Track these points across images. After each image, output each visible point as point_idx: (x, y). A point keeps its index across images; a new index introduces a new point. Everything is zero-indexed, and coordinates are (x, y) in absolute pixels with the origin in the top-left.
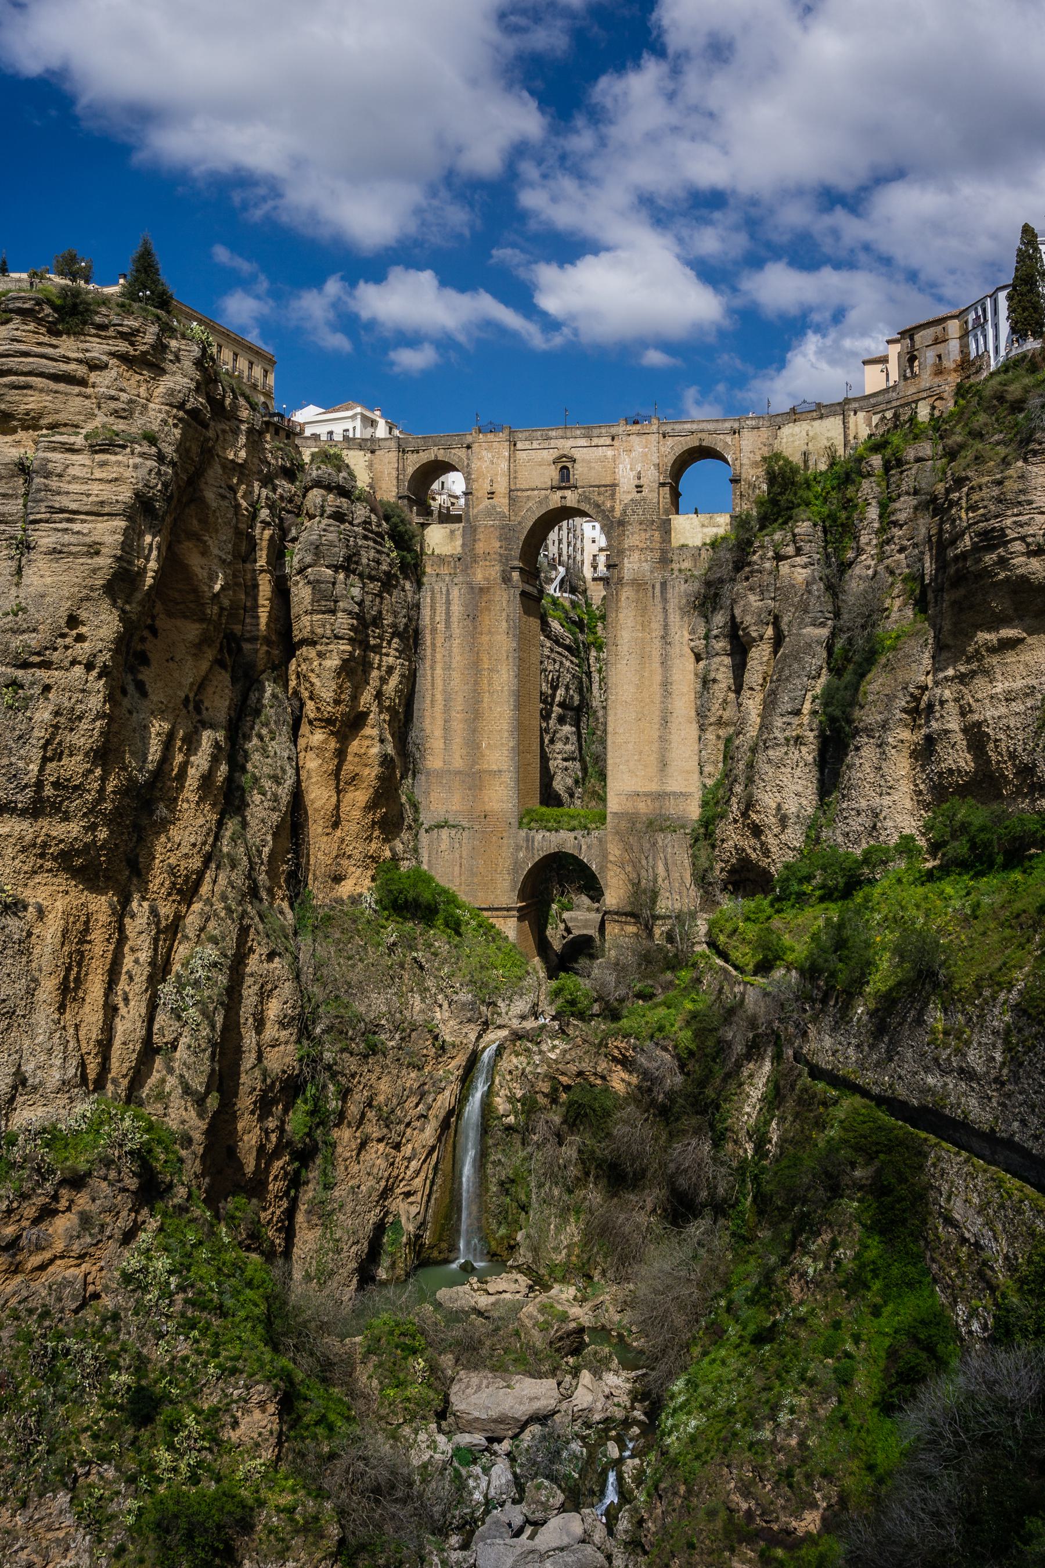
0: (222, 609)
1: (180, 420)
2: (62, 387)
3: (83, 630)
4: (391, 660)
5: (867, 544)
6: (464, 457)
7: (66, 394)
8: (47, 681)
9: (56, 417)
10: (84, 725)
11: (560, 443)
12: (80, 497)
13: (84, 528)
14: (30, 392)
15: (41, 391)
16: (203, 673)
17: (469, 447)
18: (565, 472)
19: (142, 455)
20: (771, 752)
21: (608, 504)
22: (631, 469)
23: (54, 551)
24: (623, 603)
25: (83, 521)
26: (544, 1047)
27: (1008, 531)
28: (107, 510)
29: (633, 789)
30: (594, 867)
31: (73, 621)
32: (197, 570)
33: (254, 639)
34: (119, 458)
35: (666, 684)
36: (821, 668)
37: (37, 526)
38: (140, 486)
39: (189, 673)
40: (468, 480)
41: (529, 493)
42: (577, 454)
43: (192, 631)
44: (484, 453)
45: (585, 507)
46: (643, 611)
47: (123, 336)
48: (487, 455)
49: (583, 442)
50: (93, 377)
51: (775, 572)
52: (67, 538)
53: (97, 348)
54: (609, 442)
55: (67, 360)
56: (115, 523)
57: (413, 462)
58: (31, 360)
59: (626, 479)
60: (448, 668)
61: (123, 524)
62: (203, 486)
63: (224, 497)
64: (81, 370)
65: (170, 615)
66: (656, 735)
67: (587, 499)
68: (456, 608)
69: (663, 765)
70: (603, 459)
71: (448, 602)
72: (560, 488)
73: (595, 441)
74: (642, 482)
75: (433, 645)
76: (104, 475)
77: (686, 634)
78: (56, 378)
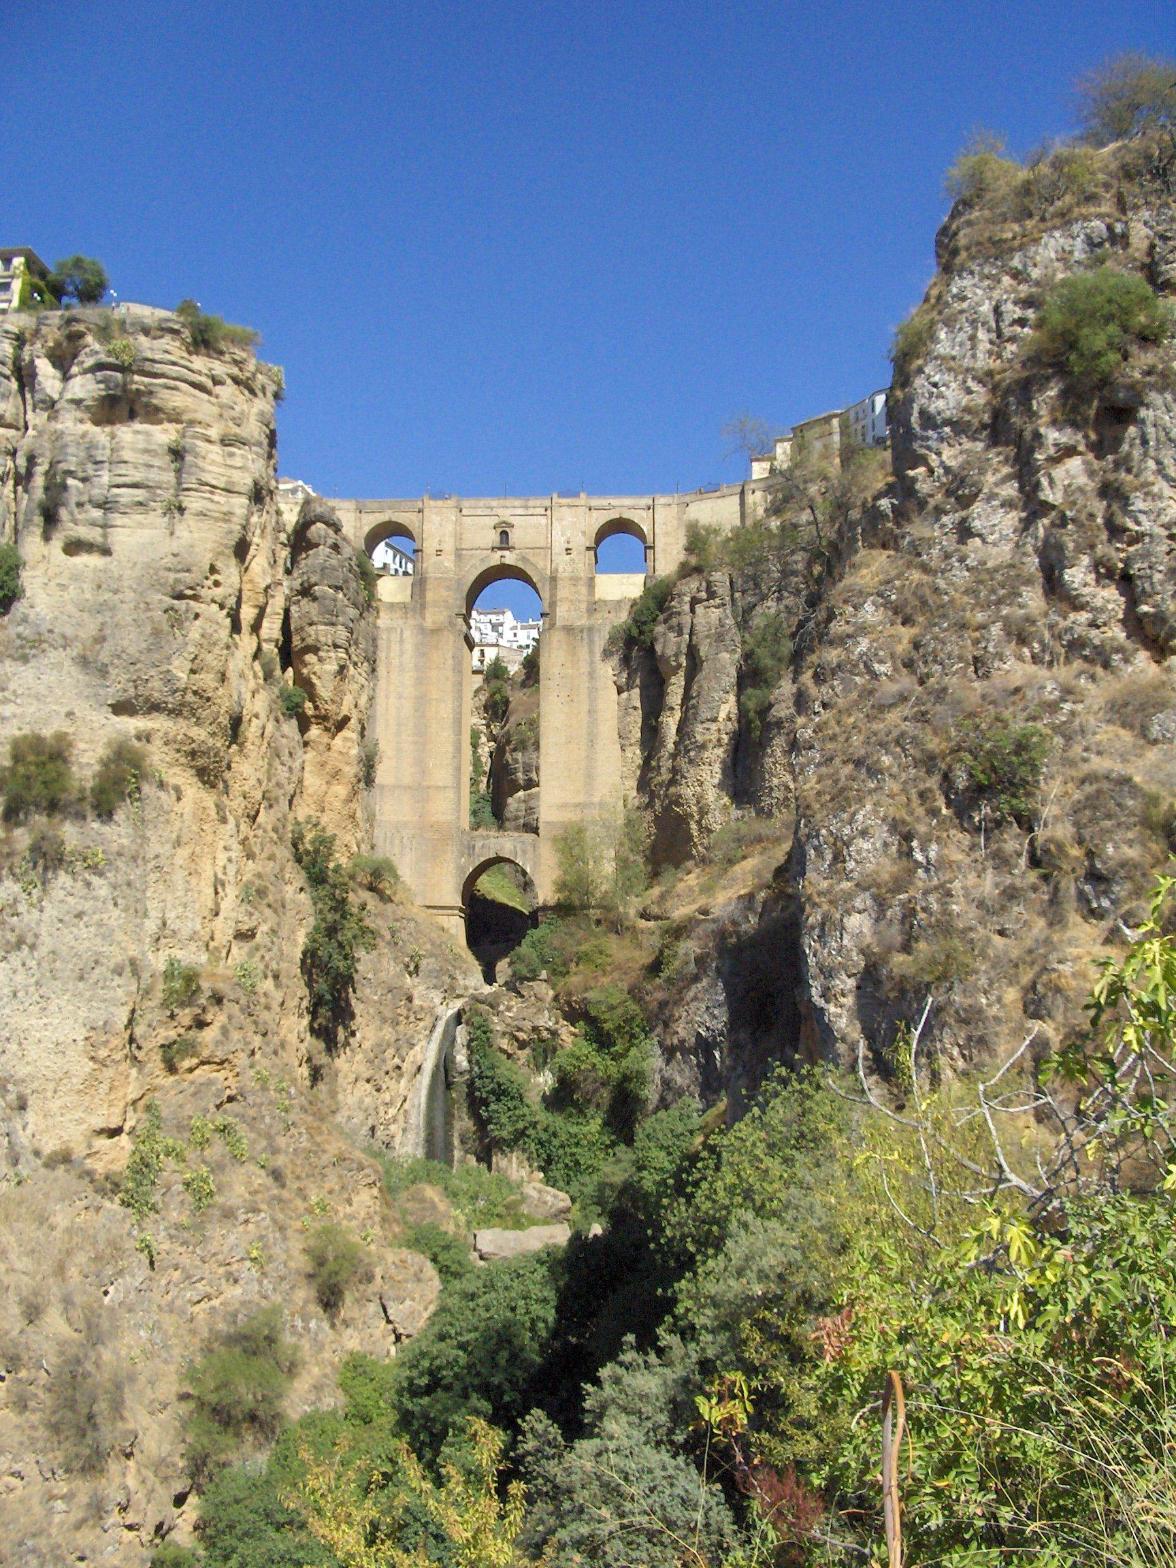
2: (197, 392)
11: (500, 512)
13: (222, 500)
15: (185, 393)
18: (504, 534)
19: (257, 454)
23: (202, 514)
24: (555, 644)
26: (502, 1008)
31: (213, 570)
42: (512, 520)
46: (573, 652)
47: (236, 362)
48: (436, 519)
50: (218, 389)
53: (220, 368)
55: (200, 373)
59: (559, 544)
64: (209, 383)
67: (524, 559)
69: (590, 776)
71: (401, 641)
72: (500, 549)
78: (195, 385)
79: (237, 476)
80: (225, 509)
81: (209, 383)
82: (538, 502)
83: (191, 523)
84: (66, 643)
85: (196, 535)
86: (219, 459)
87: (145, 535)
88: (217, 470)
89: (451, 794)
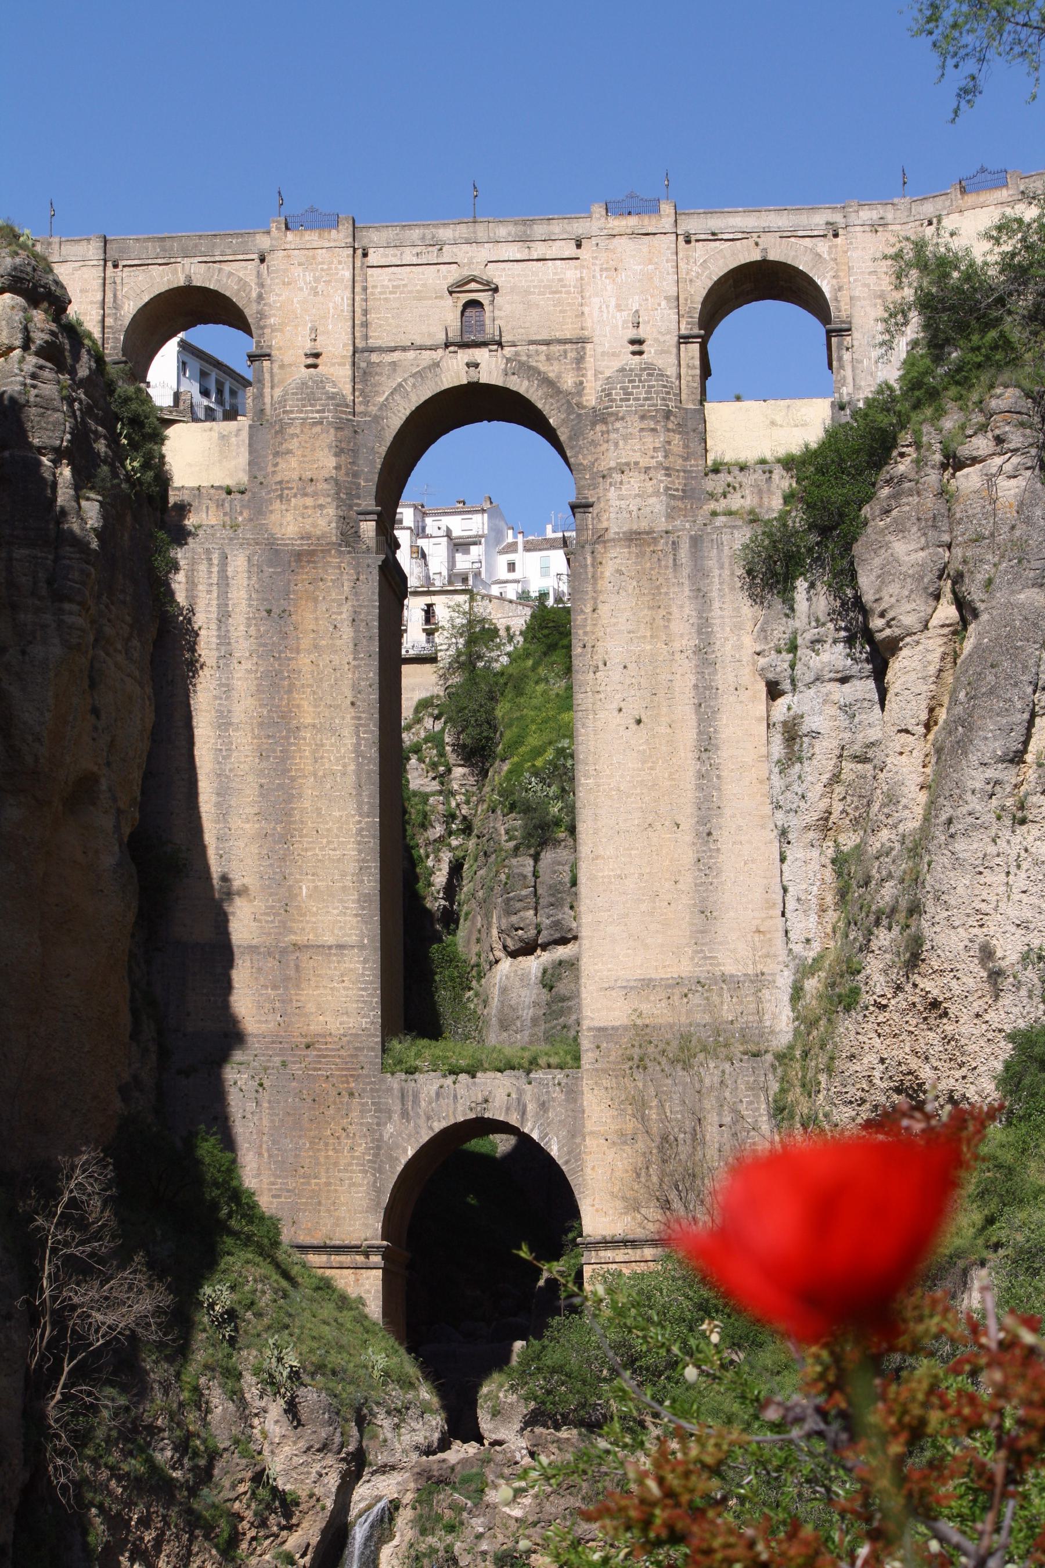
6: (252, 280)
11: (462, 253)
20: (960, 846)
22: (619, 308)
29: (639, 974)
30: (554, 1151)
41: (396, 356)
42: (497, 274)
44: (297, 271)
48: (303, 277)
49: (513, 251)
54: (570, 250)
66: (688, 856)
68: (240, 595)
73: (539, 250)
74: (642, 333)
82: (557, 228)
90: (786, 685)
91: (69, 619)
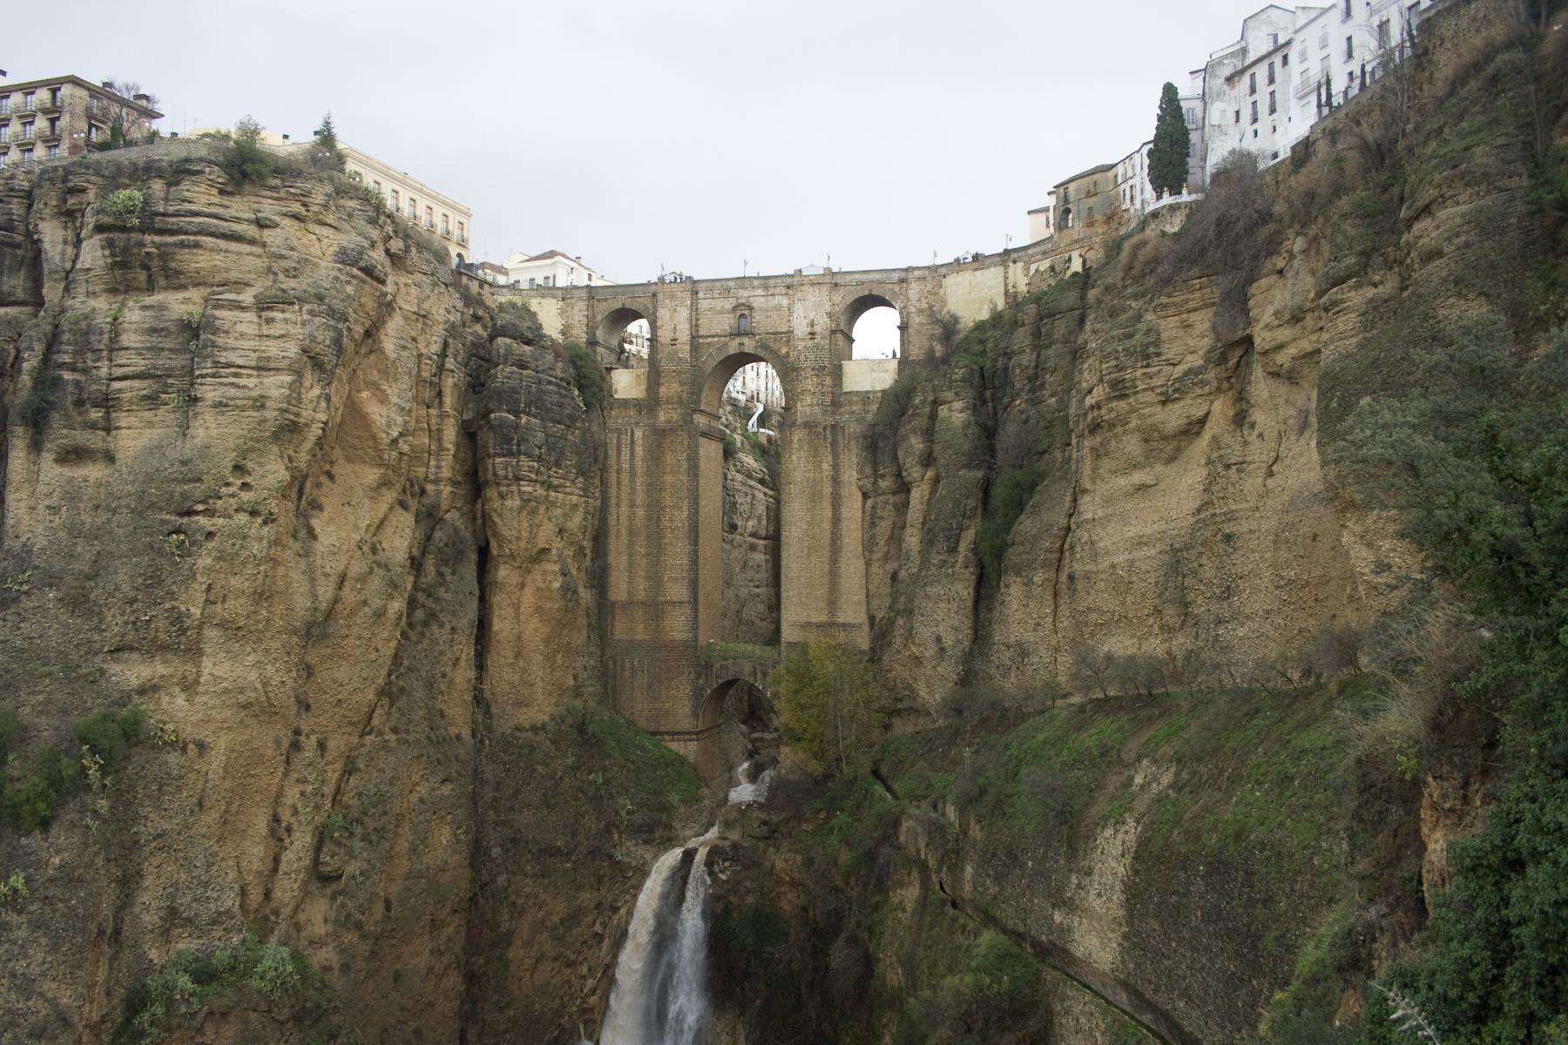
0: (401, 454)
1: (353, 277)
2: (233, 246)
3: (248, 480)
4: (574, 498)
5: (1022, 390)
7: (239, 254)
8: (212, 529)
9: (225, 275)
10: (249, 570)
12: (247, 353)
13: (251, 382)
14: (200, 252)
15: (212, 250)
16: (381, 516)
17: (654, 295)
20: (928, 589)
21: (784, 351)
23: (220, 404)
25: (250, 376)
27: (1138, 383)
28: (272, 365)
32: (376, 417)
33: (436, 481)
34: (287, 315)
35: (836, 520)
36: (976, 508)
37: (204, 380)
38: (307, 342)
39: (367, 515)
40: (654, 327)
41: (710, 340)
43: (371, 475)
45: (761, 353)
46: (815, 453)
51: (933, 417)
52: (233, 392)
53: (269, 209)
55: (238, 220)
56: (282, 378)
57: (603, 309)
58: (201, 219)
60: (632, 505)
61: (289, 379)
62: (383, 337)
63: (404, 348)
64: (251, 231)
65: (349, 460)
66: (827, 570)
67: (765, 347)
68: (639, 449)
70: (778, 308)
71: (633, 443)
72: (739, 335)
75: (619, 483)
76: (272, 332)
77: (855, 473)
79: (273, 349)
80: (254, 394)
81: (251, 231)
83: (207, 417)
84: (53, 580)
85: (214, 432)
86: (252, 330)
87: (149, 437)
88: (245, 344)
89: (687, 610)
90: (871, 494)
91: (523, 489)
